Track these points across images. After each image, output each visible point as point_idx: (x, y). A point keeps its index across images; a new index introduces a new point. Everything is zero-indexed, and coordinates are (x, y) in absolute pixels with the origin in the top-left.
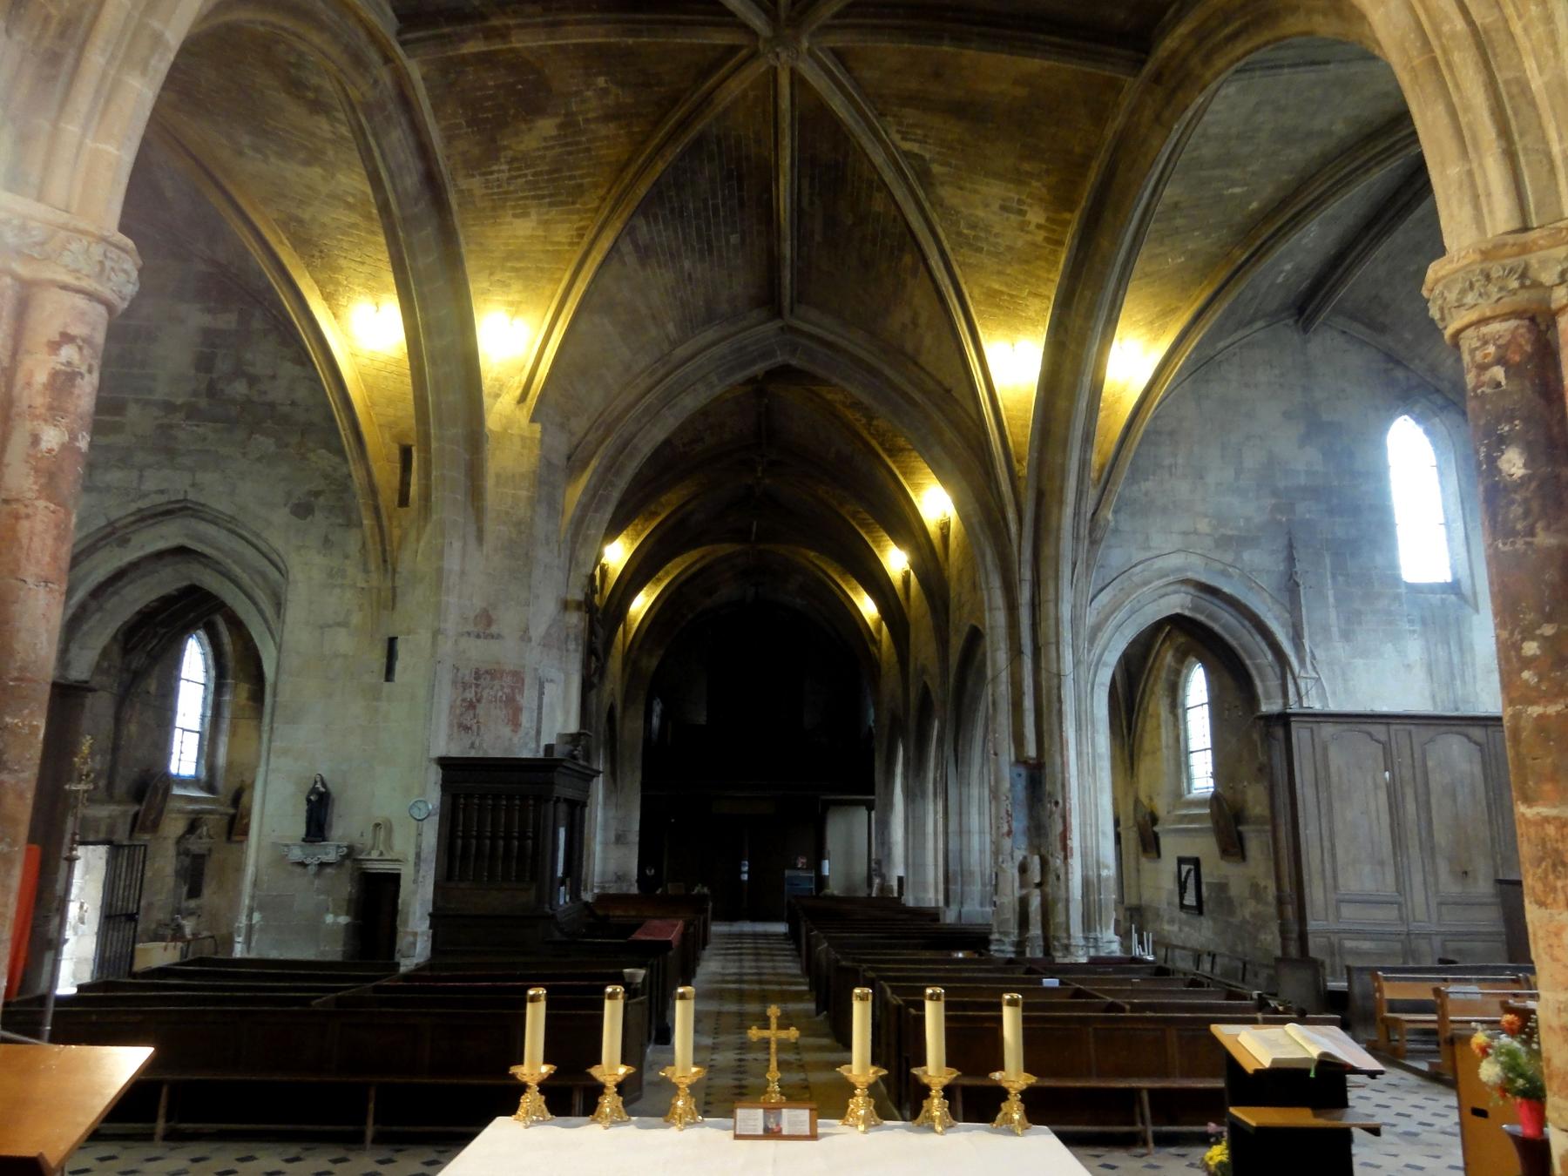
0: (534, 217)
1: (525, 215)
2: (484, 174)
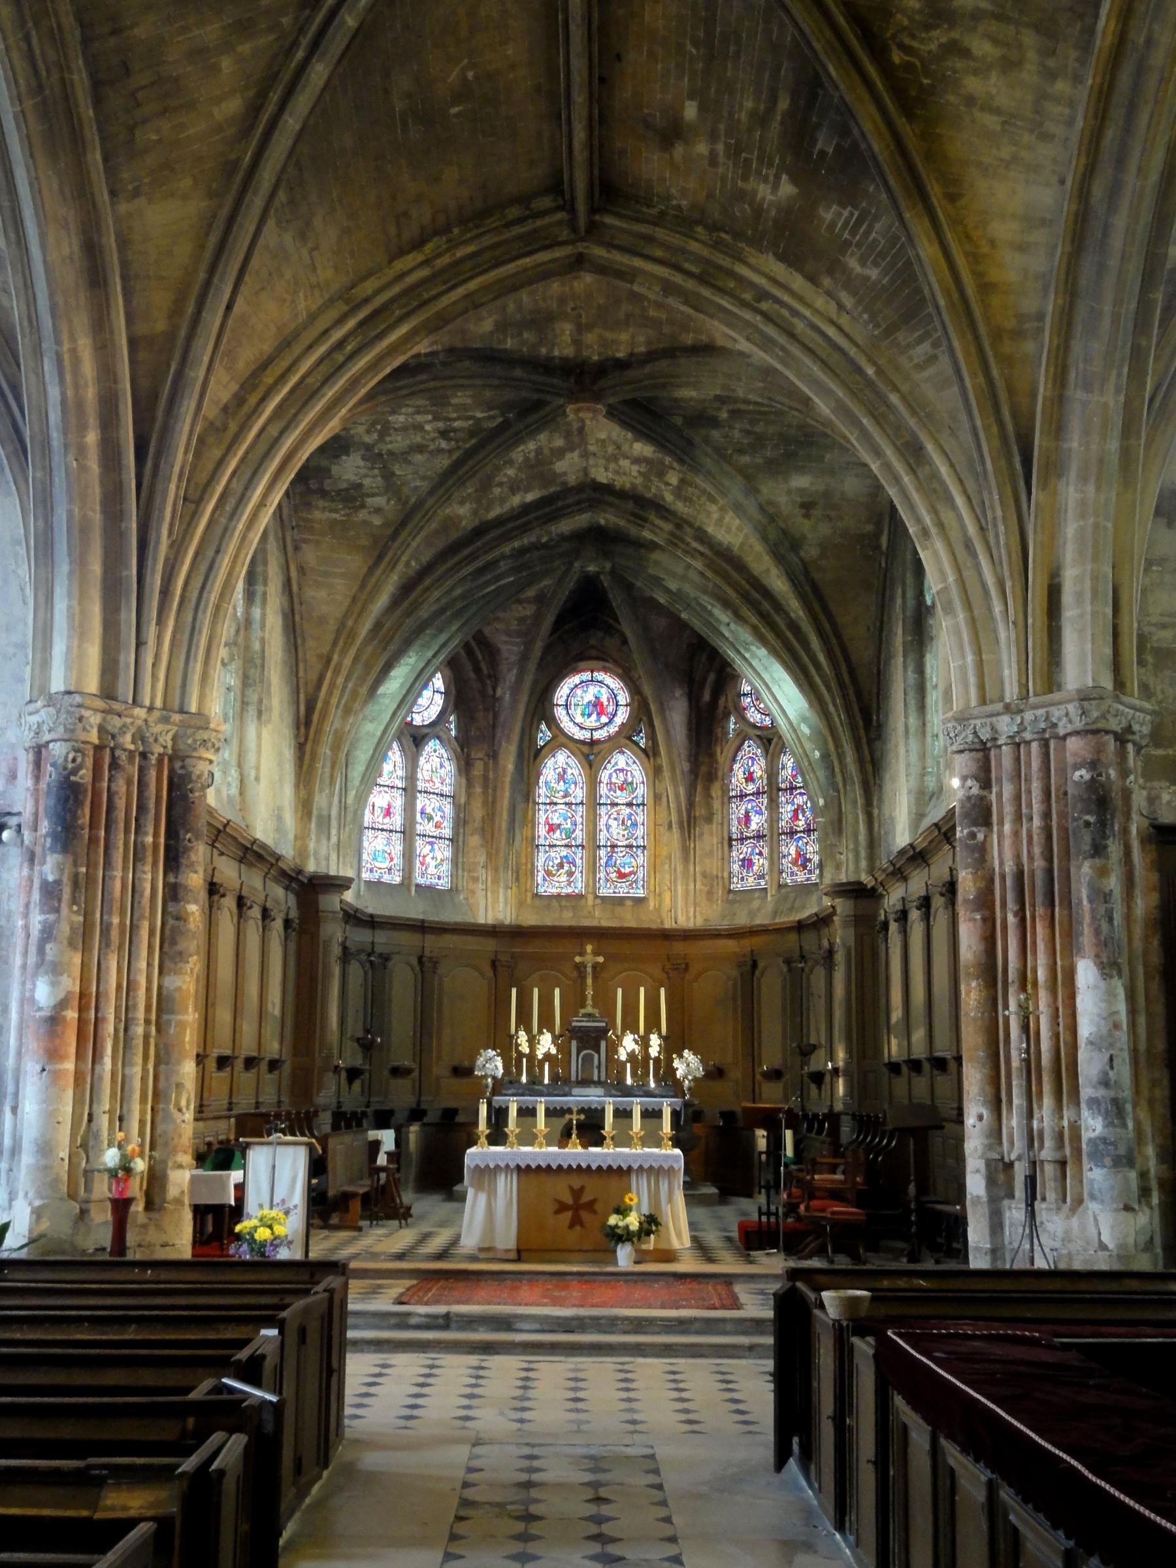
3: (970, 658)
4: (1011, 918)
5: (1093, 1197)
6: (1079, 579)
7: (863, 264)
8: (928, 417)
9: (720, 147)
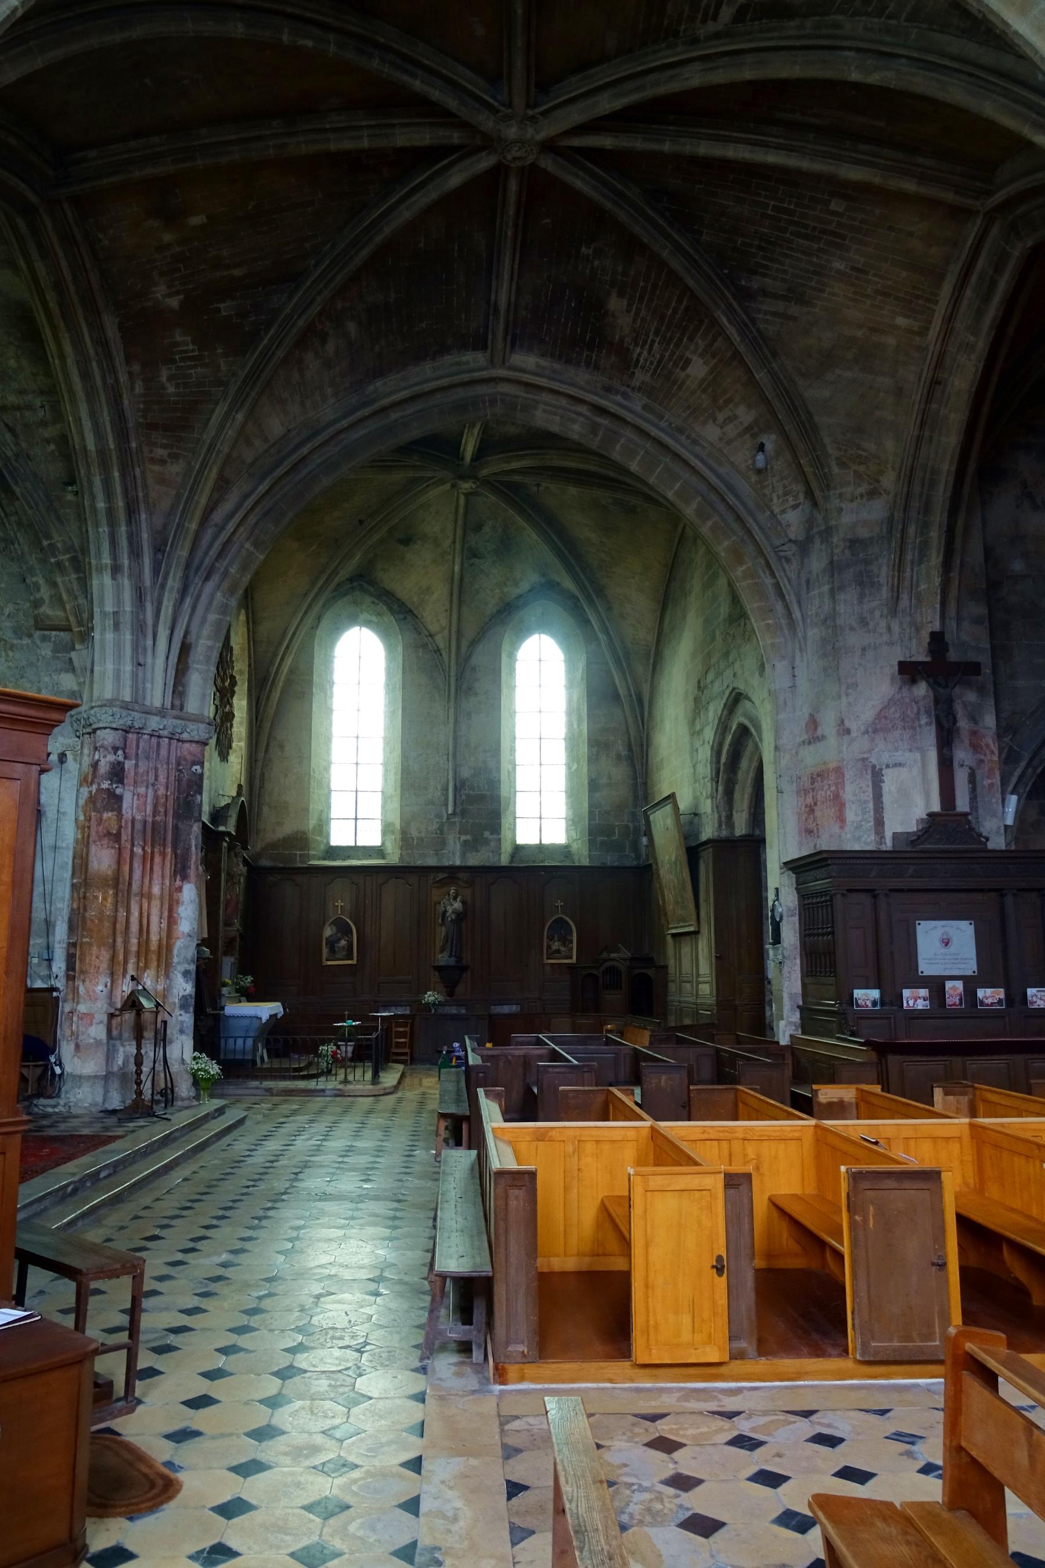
0: (695, 358)
1: (687, 362)
2: (636, 366)
3: (128, 668)
4: (138, 850)
5: (182, 1032)
6: (210, 648)
7: (170, 378)
8: (146, 495)
9: (178, 249)
